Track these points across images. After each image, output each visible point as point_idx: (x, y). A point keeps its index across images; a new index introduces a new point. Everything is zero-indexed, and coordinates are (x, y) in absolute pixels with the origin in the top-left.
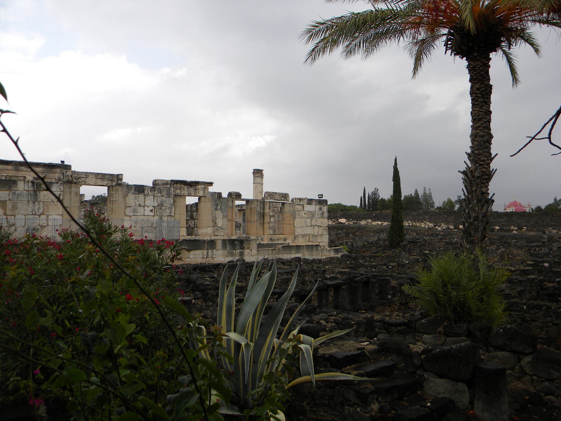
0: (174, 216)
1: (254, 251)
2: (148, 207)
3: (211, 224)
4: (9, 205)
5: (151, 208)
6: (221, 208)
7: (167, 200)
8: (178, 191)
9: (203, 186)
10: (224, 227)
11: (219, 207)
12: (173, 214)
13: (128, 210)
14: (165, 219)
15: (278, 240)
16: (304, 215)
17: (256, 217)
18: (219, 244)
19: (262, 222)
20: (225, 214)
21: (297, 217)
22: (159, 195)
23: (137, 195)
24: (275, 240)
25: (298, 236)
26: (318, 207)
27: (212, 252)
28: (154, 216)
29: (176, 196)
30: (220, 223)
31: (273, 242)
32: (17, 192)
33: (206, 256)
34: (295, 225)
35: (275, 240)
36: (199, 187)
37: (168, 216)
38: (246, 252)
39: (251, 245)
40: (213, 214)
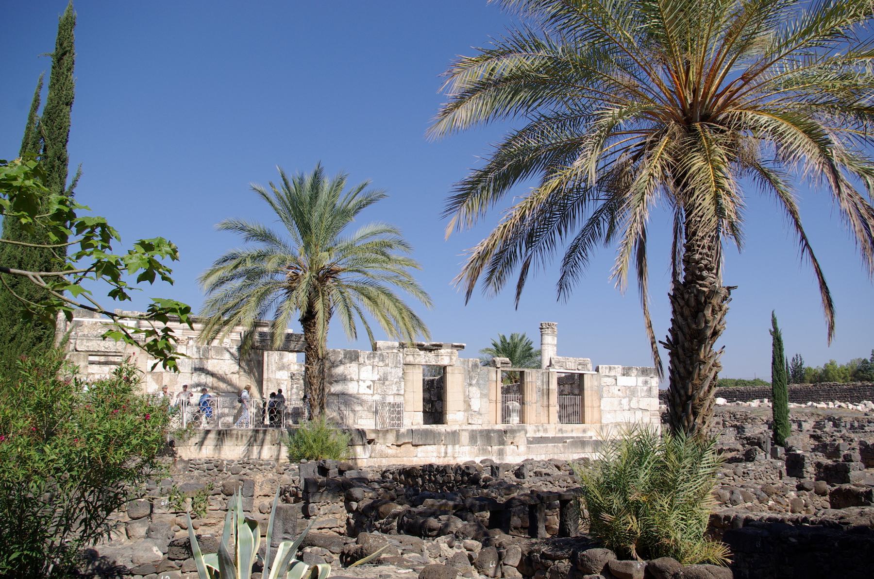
0: (403, 395)
1: (523, 448)
2: (364, 381)
3: (462, 406)
5: (369, 383)
6: (478, 383)
7: (393, 371)
8: (410, 359)
10: (483, 411)
11: (474, 382)
12: (402, 392)
16: (616, 392)
17: (534, 395)
18: (465, 437)
19: (545, 403)
20: (485, 392)
21: (605, 395)
22: (381, 364)
24: (566, 431)
25: (607, 425)
26: (641, 379)
27: (454, 449)
30: (476, 404)
33: (443, 455)
34: (602, 408)
35: (566, 431)
37: (394, 395)
38: (509, 448)
39: (516, 439)
40: (464, 392)
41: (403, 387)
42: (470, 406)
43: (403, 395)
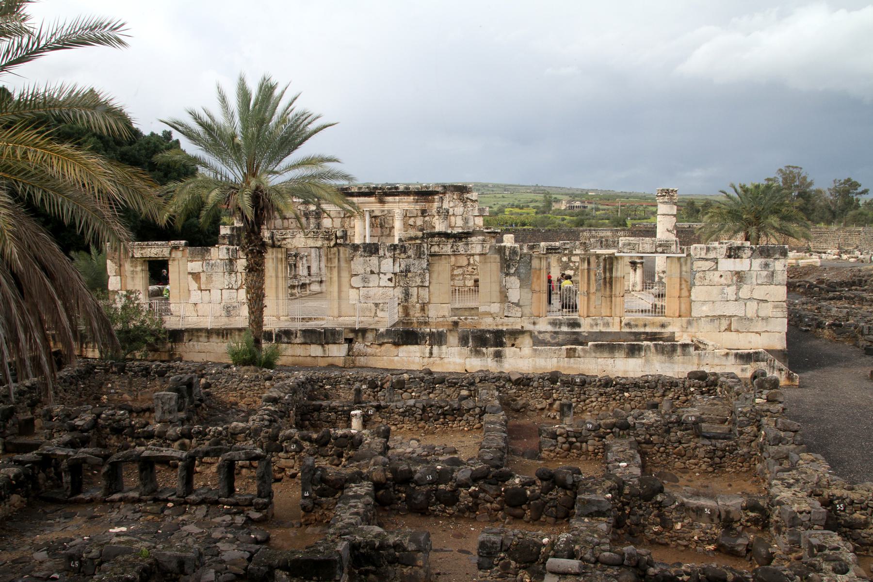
0: (428, 287)
2: (385, 274)
3: (496, 295)
4: (203, 277)
5: (389, 276)
7: (417, 262)
8: (435, 249)
9: (481, 238)
11: (512, 271)
12: (427, 284)
13: (354, 279)
14: (414, 291)
15: (645, 325)
21: (697, 282)
22: (403, 255)
23: (368, 258)
25: (700, 318)
26: (758, 262)
28: (394, 287)
29: (432, 255)
30: (514, 295)
31: (633, 330)
32: (211, 262)
33: (428, 355)
34: (693, 298)
36: (474, 239)
37: (418, 287)
39: (518, 341)
41: (427, 278)
42: (506, 297)
43: (428, 287)
